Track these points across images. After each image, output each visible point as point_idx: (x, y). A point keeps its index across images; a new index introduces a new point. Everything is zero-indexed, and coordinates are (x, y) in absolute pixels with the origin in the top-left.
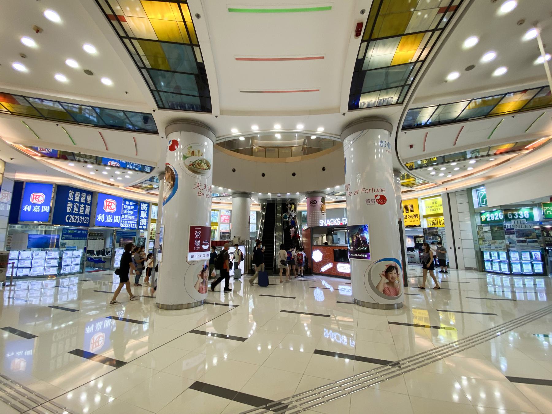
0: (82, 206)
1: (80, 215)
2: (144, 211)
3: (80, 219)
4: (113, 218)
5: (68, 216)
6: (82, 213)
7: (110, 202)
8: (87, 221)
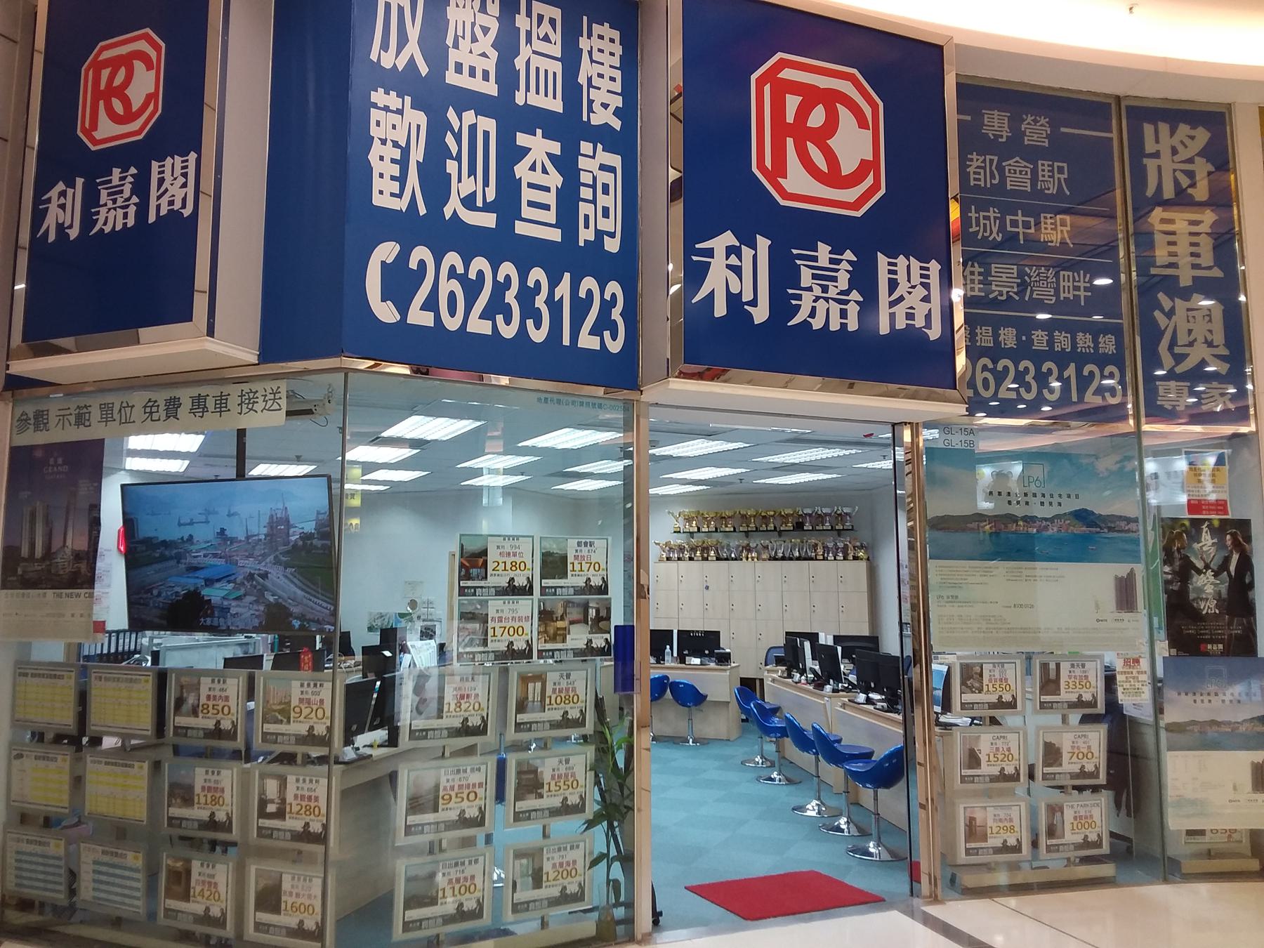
0: (539, 146)
1: (529, 253)
2: (1182, 199)
3: (527, 296)
4: (864, 280)
5: (387, 251)
6: (537, 224)
7: (811, 96)
8: (604, 324)
